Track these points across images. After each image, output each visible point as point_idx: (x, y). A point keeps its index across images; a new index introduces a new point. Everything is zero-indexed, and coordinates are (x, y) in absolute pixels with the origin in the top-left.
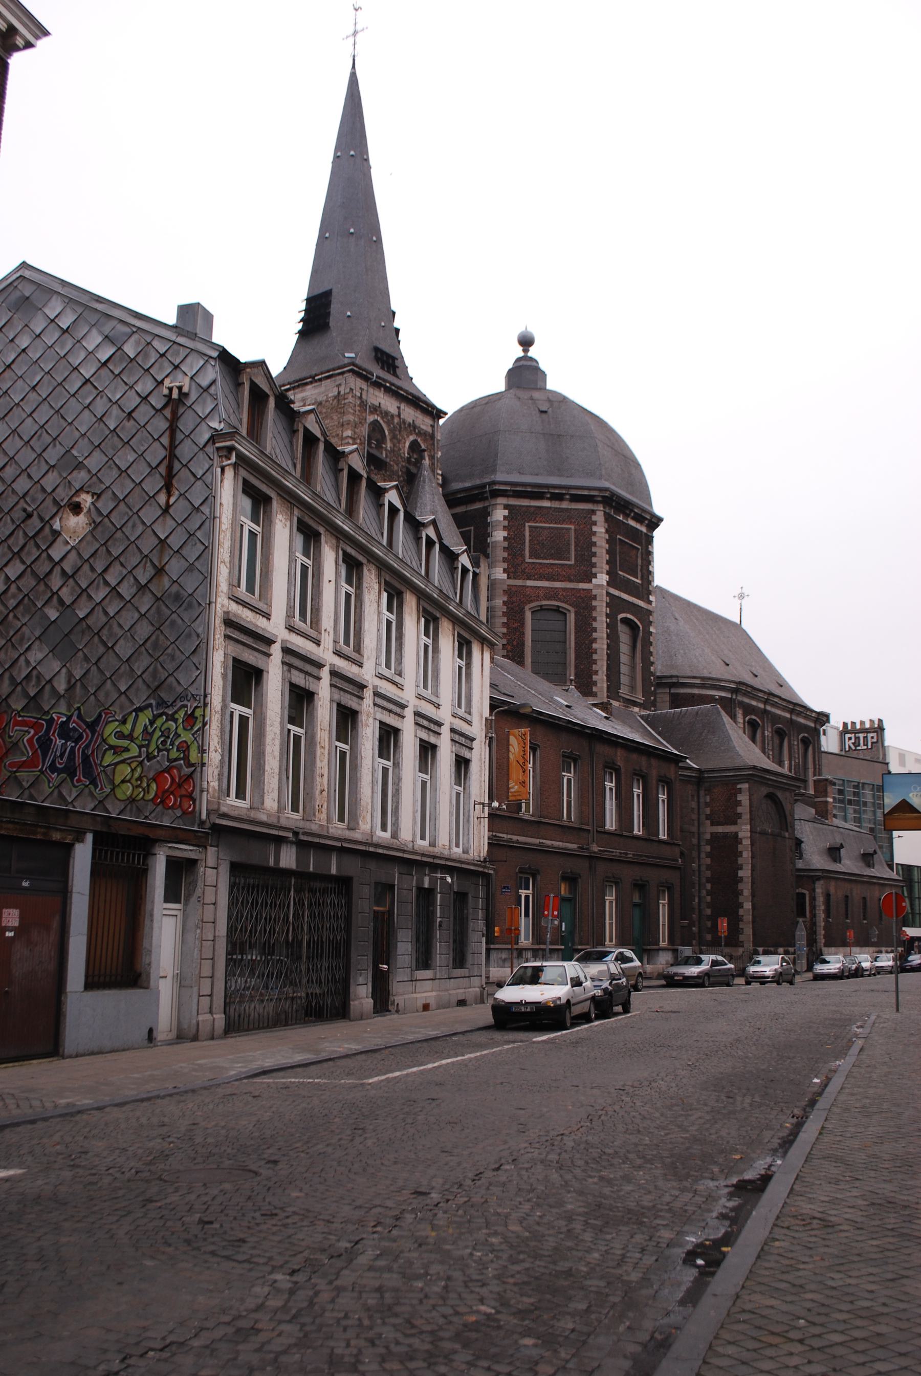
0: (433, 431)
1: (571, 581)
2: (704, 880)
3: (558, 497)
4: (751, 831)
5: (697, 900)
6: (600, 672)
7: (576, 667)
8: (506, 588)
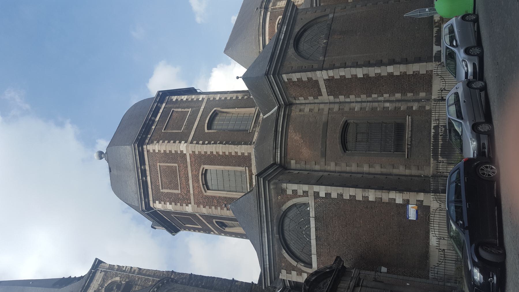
0: (104, 271)
1: (187, 167)
2: (370, 99)
3: (144, 173)
4: (322, 70)
5: (387, 105)
6: (236, 150)
7: (235, 166)
8: (196, 206)
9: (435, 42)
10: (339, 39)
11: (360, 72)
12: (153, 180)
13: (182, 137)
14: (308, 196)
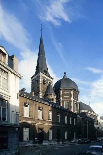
11: (88, 130)
13: (74, 98)
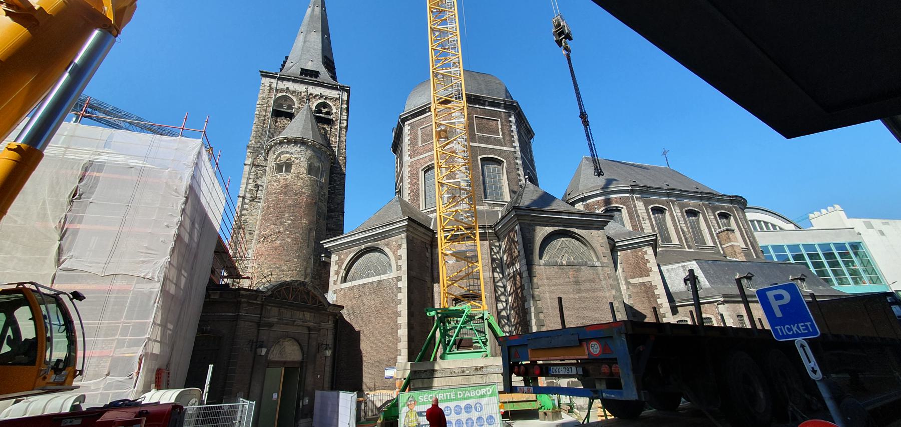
0: (340, 97)
9: (572, 381)
10: (569, 277)
12: (427, 118)
14: (397, 271)
